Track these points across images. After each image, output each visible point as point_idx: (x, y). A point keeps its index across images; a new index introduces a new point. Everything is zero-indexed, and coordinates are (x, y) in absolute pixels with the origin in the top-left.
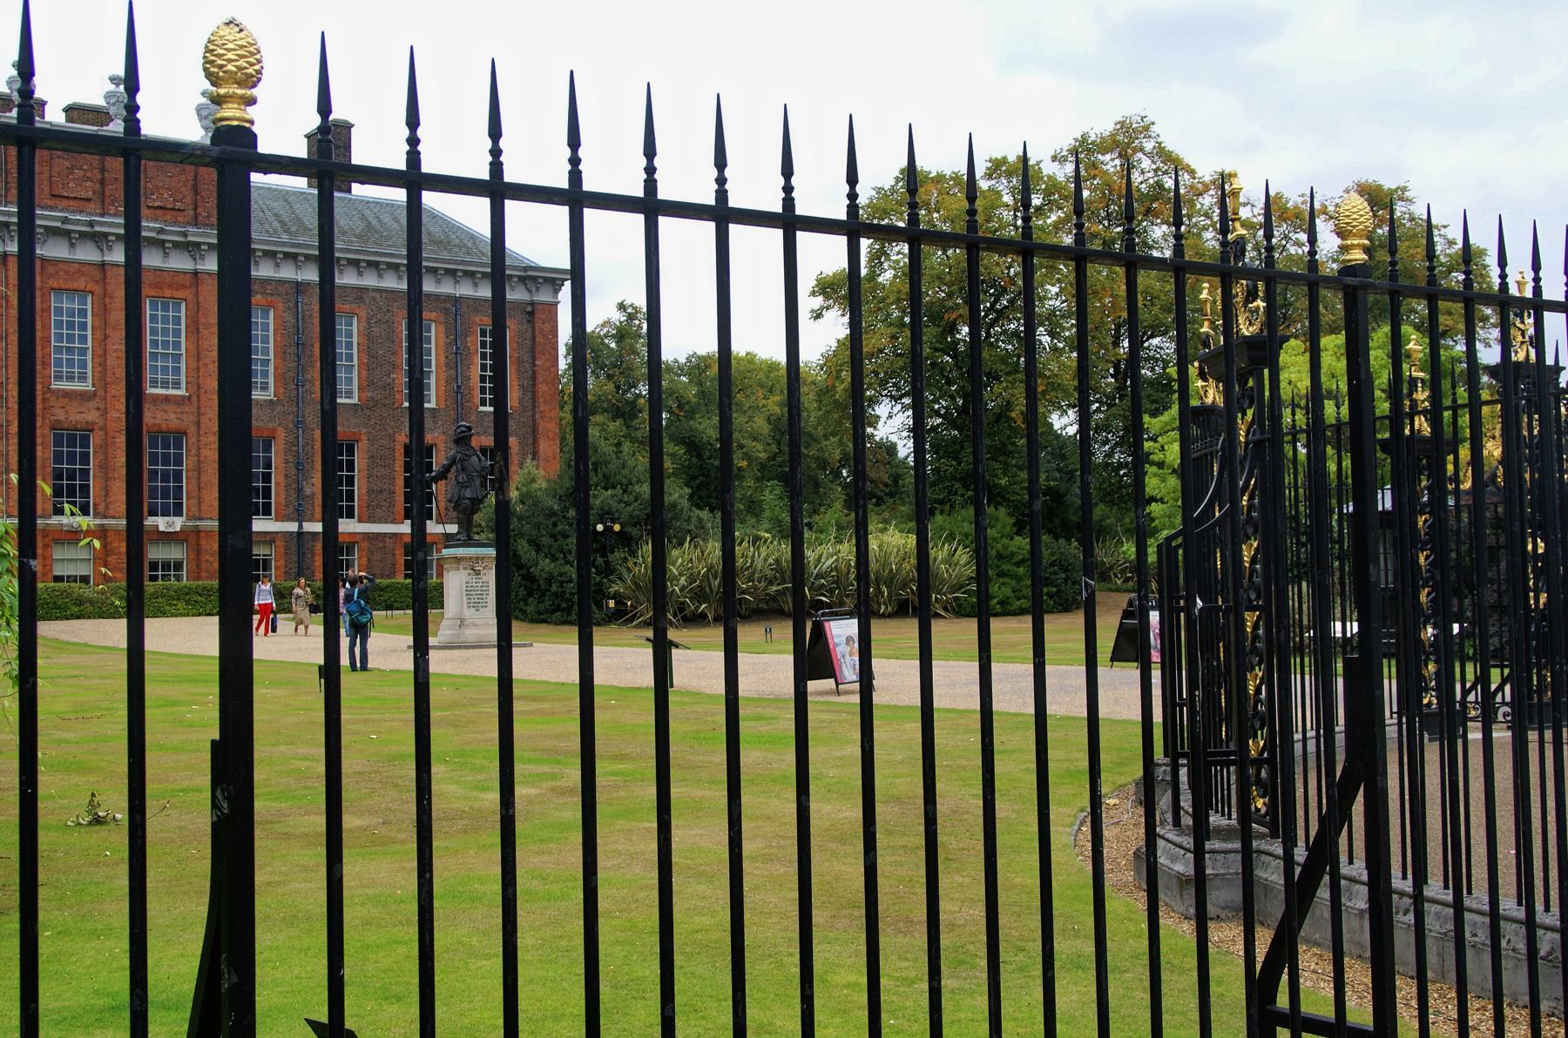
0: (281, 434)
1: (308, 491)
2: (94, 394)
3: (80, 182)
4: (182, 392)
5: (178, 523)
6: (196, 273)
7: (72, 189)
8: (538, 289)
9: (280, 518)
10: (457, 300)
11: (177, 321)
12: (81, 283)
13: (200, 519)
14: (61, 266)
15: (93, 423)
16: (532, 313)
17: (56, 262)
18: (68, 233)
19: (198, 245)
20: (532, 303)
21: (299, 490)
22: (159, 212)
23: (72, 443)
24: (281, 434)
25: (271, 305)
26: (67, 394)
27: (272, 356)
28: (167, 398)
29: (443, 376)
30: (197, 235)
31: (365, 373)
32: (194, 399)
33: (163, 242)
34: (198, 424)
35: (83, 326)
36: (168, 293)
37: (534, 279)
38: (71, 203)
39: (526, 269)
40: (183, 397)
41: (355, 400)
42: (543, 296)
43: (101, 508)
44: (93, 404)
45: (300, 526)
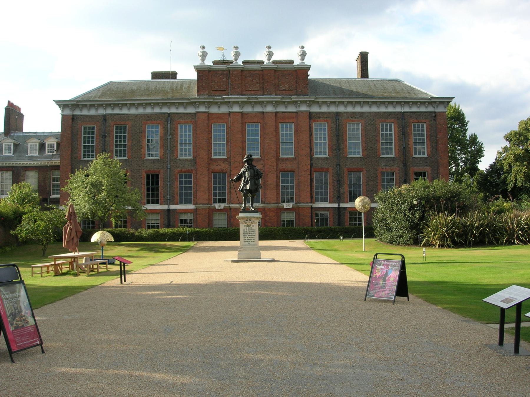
0: (331, 170)
1: (342, 191)
2: (261, 159)
4: (293, 156)
5: (291, 205)
6: (297, 112)
9: (331, 202)
10: (403, 114)
11: (291, 130)
13: (299, 203)
17: (247, 113)
18: (250, 103)
19: (297, 101)
20: (435, 113)
21: (339, 191)
22: (284, 92)
24: (331, 170)
25: (326, 121)
27: (327, 141)
30: (295, 98)
31: (364, 145)
33: (284, 102)
34: (298, 167)
36: (287, 120)
37: (435, 102)
38: (253, 92)
41: (361, 156)
43: (263, 200)
44: (261, 162)
45: (339, 205)
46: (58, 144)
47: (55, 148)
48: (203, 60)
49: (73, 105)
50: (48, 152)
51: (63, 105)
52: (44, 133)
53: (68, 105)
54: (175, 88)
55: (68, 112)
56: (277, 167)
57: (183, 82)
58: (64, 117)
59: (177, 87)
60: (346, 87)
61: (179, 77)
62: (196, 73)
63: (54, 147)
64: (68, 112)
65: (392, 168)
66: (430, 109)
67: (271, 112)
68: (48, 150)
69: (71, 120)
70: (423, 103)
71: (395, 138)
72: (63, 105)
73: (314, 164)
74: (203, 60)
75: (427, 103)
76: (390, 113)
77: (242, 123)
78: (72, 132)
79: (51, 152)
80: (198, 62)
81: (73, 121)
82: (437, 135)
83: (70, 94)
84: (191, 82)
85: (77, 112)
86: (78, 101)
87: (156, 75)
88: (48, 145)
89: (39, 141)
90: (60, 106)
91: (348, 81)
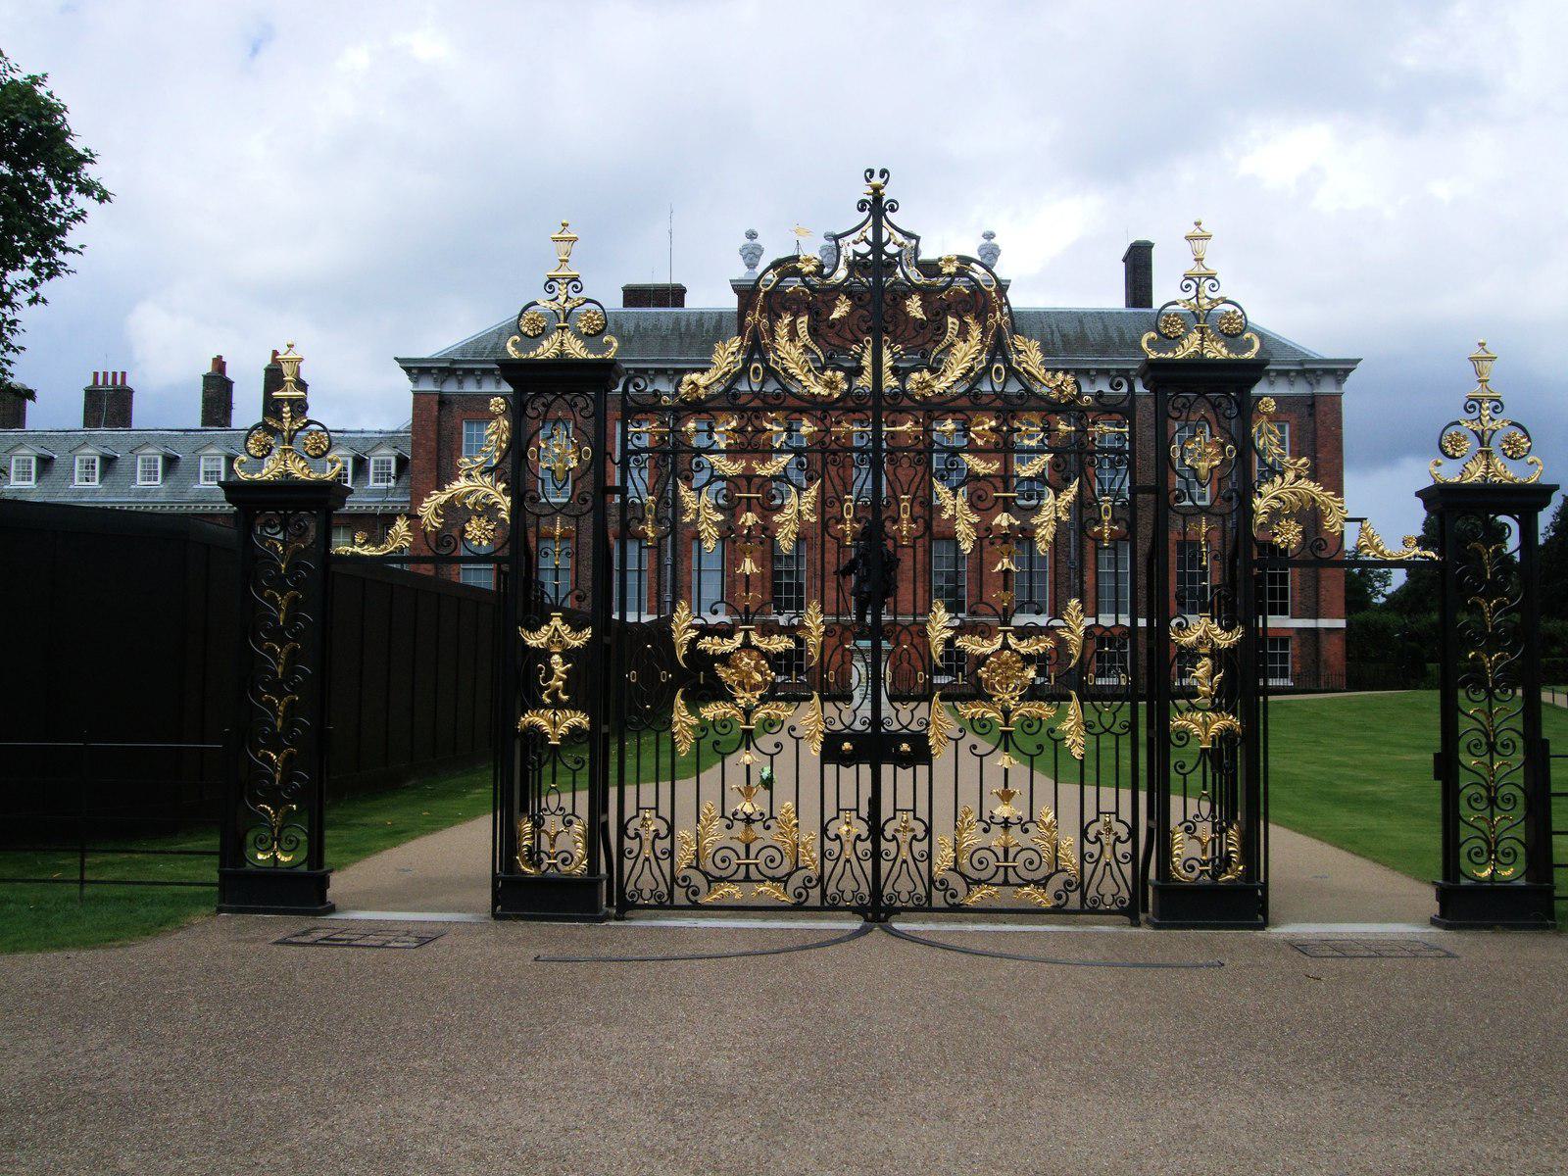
8: (1318, 382)
16: (1312, 406)
20: (1313, 397)
37: (1313, 371)
39: (1301, 363)
42: (1327, 387)
46: (402, 463)
47: (393, 471)
48: (751, 266)
49: (441, 369)
50: (376, 481)
51: (416, 369)
52: (362, 432)
53: (430, 369)
54: (683, 330)
55: (428, 386)
57: (701, 316)
58: (415, 393)
59: (688, 325)
60: (1094, 333)
61: (693, 302)
62: (735, 297)
63: (389, 468)
64: (428, 386)
66: (1301, 388)
68: (376, 474)
69: (436, 407)
70: (1285, 373)
72: (416, 369)
74: (751, 266)
75: (1292, 374)
78: (439, 433)
79: (382, 481)
80: (741, 272)
81: (440, 410)
82: (1316, 453)
83: (435, 344)
84: (721, 315)
85: (451, 388)
86: (454, 362)
87: (635, 296)
88: (376, 462)
89: (353, 453)
90: (408, 370)
91: (1101, 316)
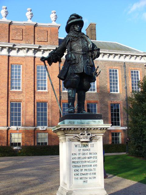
3: (19, 36)
4: (46, 91)
7: (17, 38)
12: (19, 62)
14: (14, 58)
15: (22, 100)
22: (40, 42)
23: (16, 106)
26: (14, 92)
28: (42, 92)
29: (121, 84)
32: (50, 92)
35: (19, 74)
38: (17, 41)
40: (46, 92)
44: (22, 95)
56: (34, 99)
65: (118, 101)
67: (31, 57)
71: (119, 80)
73: (62, 97)
76: (116, 62)
77: (8, 64)
